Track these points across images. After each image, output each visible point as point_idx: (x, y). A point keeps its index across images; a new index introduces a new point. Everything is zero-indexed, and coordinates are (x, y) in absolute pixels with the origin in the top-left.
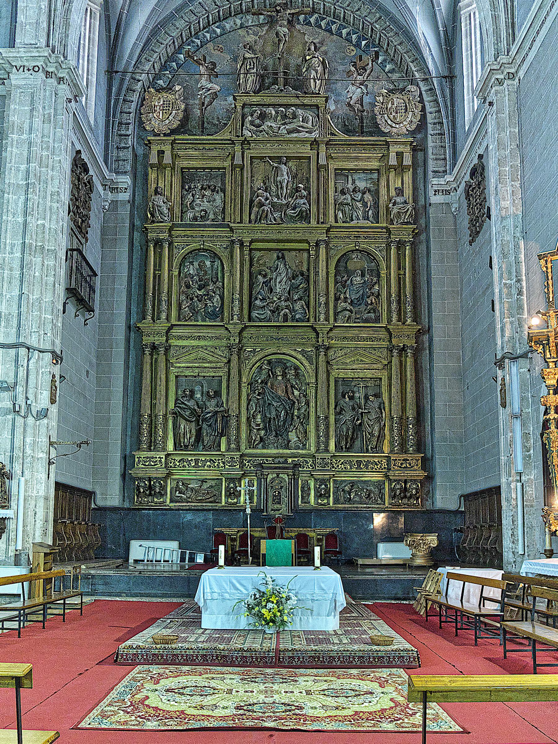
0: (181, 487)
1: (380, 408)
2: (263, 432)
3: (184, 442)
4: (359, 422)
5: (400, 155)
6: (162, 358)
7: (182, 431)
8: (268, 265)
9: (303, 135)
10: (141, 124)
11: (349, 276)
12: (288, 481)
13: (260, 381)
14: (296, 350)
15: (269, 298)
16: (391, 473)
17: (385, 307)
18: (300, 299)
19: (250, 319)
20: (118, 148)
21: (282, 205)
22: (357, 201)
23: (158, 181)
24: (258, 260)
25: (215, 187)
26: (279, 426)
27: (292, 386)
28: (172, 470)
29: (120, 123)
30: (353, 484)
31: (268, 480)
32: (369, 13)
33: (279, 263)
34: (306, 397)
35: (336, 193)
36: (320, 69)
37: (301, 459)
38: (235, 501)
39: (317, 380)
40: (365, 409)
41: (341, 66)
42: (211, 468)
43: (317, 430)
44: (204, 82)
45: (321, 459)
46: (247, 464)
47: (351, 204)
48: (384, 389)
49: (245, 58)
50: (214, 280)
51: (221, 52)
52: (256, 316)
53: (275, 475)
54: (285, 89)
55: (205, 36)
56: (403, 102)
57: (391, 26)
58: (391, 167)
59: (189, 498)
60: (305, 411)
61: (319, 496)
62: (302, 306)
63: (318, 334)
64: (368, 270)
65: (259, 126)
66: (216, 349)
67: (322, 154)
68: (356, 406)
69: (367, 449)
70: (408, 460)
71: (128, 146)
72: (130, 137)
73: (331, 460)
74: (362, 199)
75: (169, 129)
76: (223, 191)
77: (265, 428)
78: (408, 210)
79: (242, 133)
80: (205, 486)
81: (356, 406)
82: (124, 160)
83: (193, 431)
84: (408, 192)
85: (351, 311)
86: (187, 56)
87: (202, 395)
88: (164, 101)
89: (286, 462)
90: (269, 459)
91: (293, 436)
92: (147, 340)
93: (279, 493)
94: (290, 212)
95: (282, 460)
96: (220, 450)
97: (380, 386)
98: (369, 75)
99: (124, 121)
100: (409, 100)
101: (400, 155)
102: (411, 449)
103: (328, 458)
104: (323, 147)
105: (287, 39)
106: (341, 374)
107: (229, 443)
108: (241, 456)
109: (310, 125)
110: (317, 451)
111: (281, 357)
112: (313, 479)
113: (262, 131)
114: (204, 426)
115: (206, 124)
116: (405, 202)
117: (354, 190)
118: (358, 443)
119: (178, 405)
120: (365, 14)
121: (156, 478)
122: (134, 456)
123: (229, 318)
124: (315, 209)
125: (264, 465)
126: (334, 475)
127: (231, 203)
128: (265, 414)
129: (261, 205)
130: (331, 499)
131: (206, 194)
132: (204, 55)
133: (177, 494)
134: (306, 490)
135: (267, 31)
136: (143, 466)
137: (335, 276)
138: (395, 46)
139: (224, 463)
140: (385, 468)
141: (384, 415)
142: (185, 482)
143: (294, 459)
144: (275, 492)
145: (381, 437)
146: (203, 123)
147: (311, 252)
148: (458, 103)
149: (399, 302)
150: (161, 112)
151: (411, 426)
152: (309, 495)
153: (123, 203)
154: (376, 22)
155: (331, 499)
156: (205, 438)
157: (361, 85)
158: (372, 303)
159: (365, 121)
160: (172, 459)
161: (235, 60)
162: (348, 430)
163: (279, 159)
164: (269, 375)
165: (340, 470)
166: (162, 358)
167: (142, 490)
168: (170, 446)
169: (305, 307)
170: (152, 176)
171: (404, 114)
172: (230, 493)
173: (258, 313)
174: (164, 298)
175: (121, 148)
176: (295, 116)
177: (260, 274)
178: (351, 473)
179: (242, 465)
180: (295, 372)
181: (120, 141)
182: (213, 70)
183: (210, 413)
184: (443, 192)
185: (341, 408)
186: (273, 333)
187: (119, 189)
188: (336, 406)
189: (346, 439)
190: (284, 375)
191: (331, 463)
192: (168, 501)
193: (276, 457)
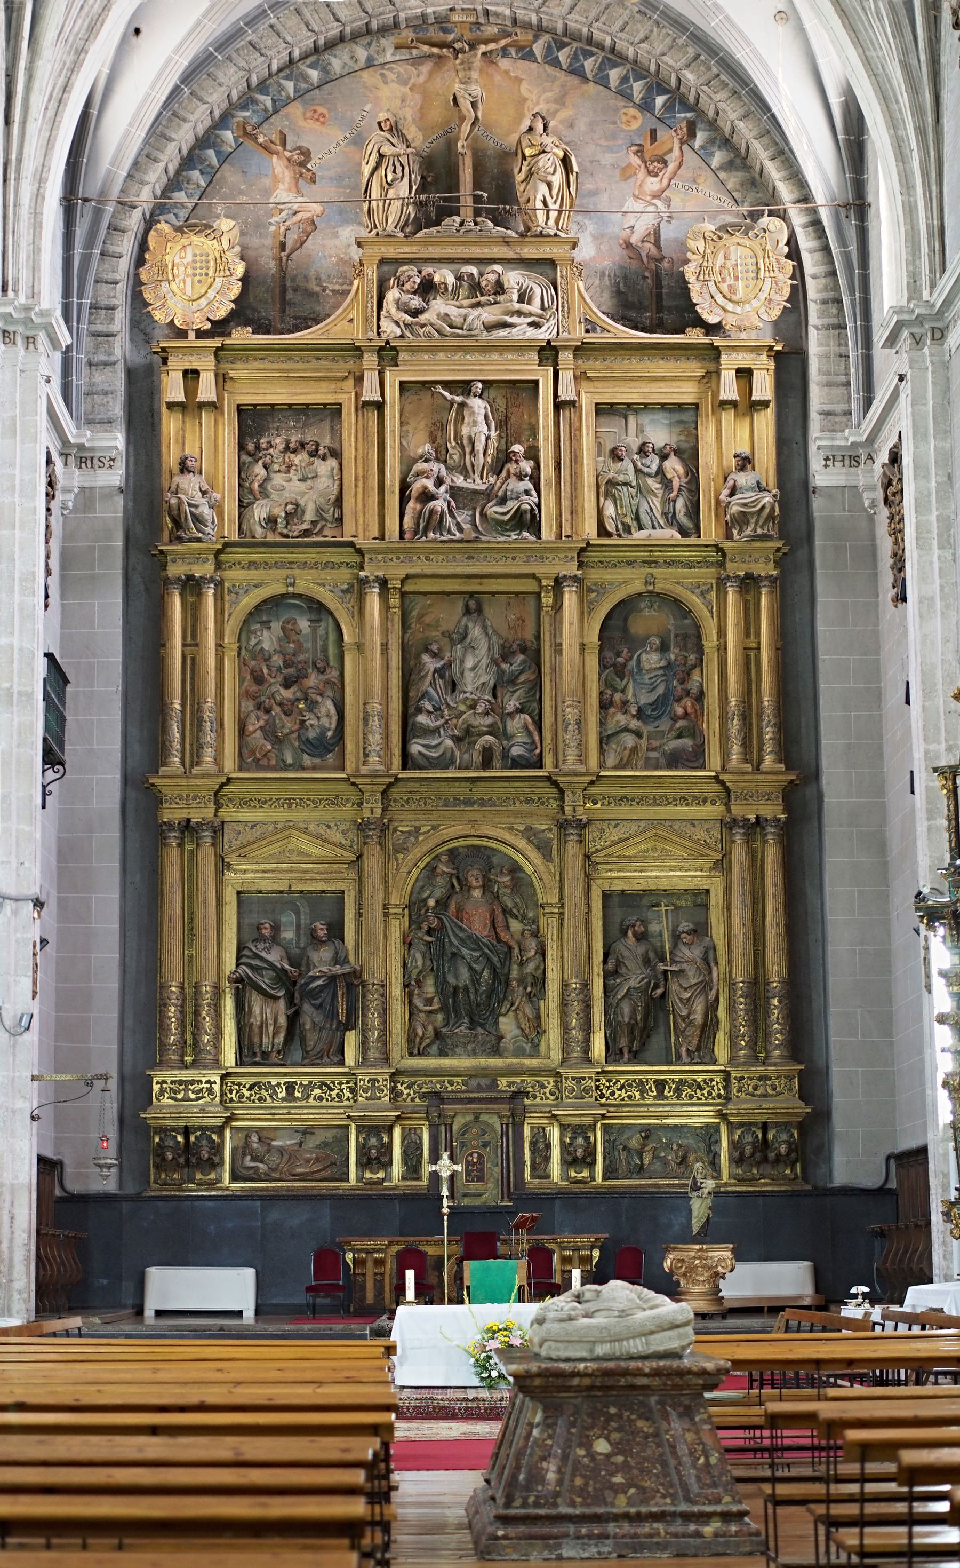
0: (255, 1145)
1: (705, 959)
2: (440, 1017)
3: (261, 1045)
4: (659, 991)
5: (744, 374)
6: (207, 855)
7: (256, 1020)
8: (444, 627)
9: (522, 331)
10: (138, 301)
11: (632, 651)
12: (499, 1129)
13: (431, 903)
14: (512, 829)
15: (448, 706)
16: (731, 1109)
17: (716, 726)
18: (520, 710)
19: (407, 761)
20: (90, 364)
21: (475, 492)
22: (649, 475)
23: (184, 437)
24: (421, 617)
25: (317, 445)
26: (478, 1005)
27: (505, 911)
28: (236, 1108)
29: (94, 307)
30: (648, 1133)
31: (455, 1127)
32: (671, 48)
33: (470, 625)
34: (536, 936)
35: (599, 455)
36: (557, 179)
37: (529, 1079)
38: (381, 1175)
39: (562, 898)
40: (673, 962)
41: (608, 156)
42: (324, 1103)
43: (564, 1014)
44: (283, 194)
45: (573, 1079)
46: (406, 1092)
47: (634, 483)
48: (715, 916)
49: (381, 156)
50: (320, 665)
51: (323, 123)
52: (420, 753)
53: (470, 1118)
54: (476, 224)
55: (282, 88)
56: (751, 253)
57: (723, 77)
58: (724, 404)
59: (274, 1170)
60: (537, 968)
61: (570, 1161)
62: (526, 727)
63: (562, 792)
64: (676, 636)
65: (415, 313)
66: (329, 827)
67: (566, 376)
68: (651, 955)
69: (679, 1057)
70: (770, 1079)
71: (113, 358)
72: (118, 338)
73: (598, 1080)
74: (660, 471)
75: (208, 319)
76: (336, 453)
77: (444, 1008)
78: (763, 507)
79: (379, 327)
80: (312, 1142)
81: (651, 955)
82: (106, 393)
83: (282, 1021)
84: (766, 457)
85: (638, 734)
86: (241, 133)
87: (298, 935)
88: (195, 255)
89: (494, 1084)
90: (455, 1079)
91: (507, 1025)
92: (172, 813)
93: (480, 1156)
94: (493, 510)
95: (484, 1082)
96: (342, 1063)
97: (706, 906)
98: (675, 174)
99: (104, 301)
100: (764, 250)
101: (744, 374)
102: (777, 1053)
103: (590, 1078)
104: (566, 358)
105: (480, 114)
106: (616, 881)
107: (364, 1045)
108: (393, 1075)
109: (535, 307)
110: (564, 1061)
111: (478, 842)
112: (555, 1124)
113: (423, 326)
114: (307, 1007)
115: (290, 295)
116: (760, 488)
117: (642, 450)
118: (657, 1041)
119: (243, 960)
120: (659, 50)
121: (200, 1128)
122: (150, 1079)
123: (357, 759)
124: (553, 504)
125: (445, 1095)
126: (603, 1115)
127: (356, 486)
128: (445, 978)
129: (426, 497)
130: (599, 1167)
131: (297, 462)
132: (281, 132)
133: (248, 1162)
134: (542, 1150)
135: (431, 74)
136: (170, 1102)
137: (600, 651)
138: (732, 122)
139: (352, 1091)
140: (719, 1096)
141: (715, 974)
142: (264, 1134)
143: (512, 1079)
144: (471, 1155)
145: (709, 1027)
146: (284, 290)
147: (543, 600)
148: (873, 263)
149: (745, 717)
150: (189, 280)
151: (775, 1002)
152: (547, 1159)
153: (107, 494)
154: (688, 66)
155: (599, 1167)
156: (308, 1035)
157: (654, 197)
158: (686, 715)
159: (664, 283)
160: (233, 1083)
161: (358, 141)
162: (634, 1011)
163: (465, 387)
164: (453, 886)
165: (618, 1101)
166: (207, 855)
167: (170, 1156)
168: (229, 1056)
169: (532, 728)
170: (170, 424)
171: (752, 283)
172: (370, 1159)
173: (424, 746)
174: (207, 715)
175: (97, 365)
176: (499, 288)
177: (427, 650)
178: (642, 1109)
179: (395, 1094)
180: (512, 879)
181: (97, 346)
182: (305, 167)
183: (319, 978)
184: (843, 461)
185: (617, 960)
186: (462, 790)
187: (96, 461)
188: (606, 956)
189: (631, 1032)
190: (486, 887)
191: (597, 1087)
192: (227, 1176)
193: (470, 1076)
